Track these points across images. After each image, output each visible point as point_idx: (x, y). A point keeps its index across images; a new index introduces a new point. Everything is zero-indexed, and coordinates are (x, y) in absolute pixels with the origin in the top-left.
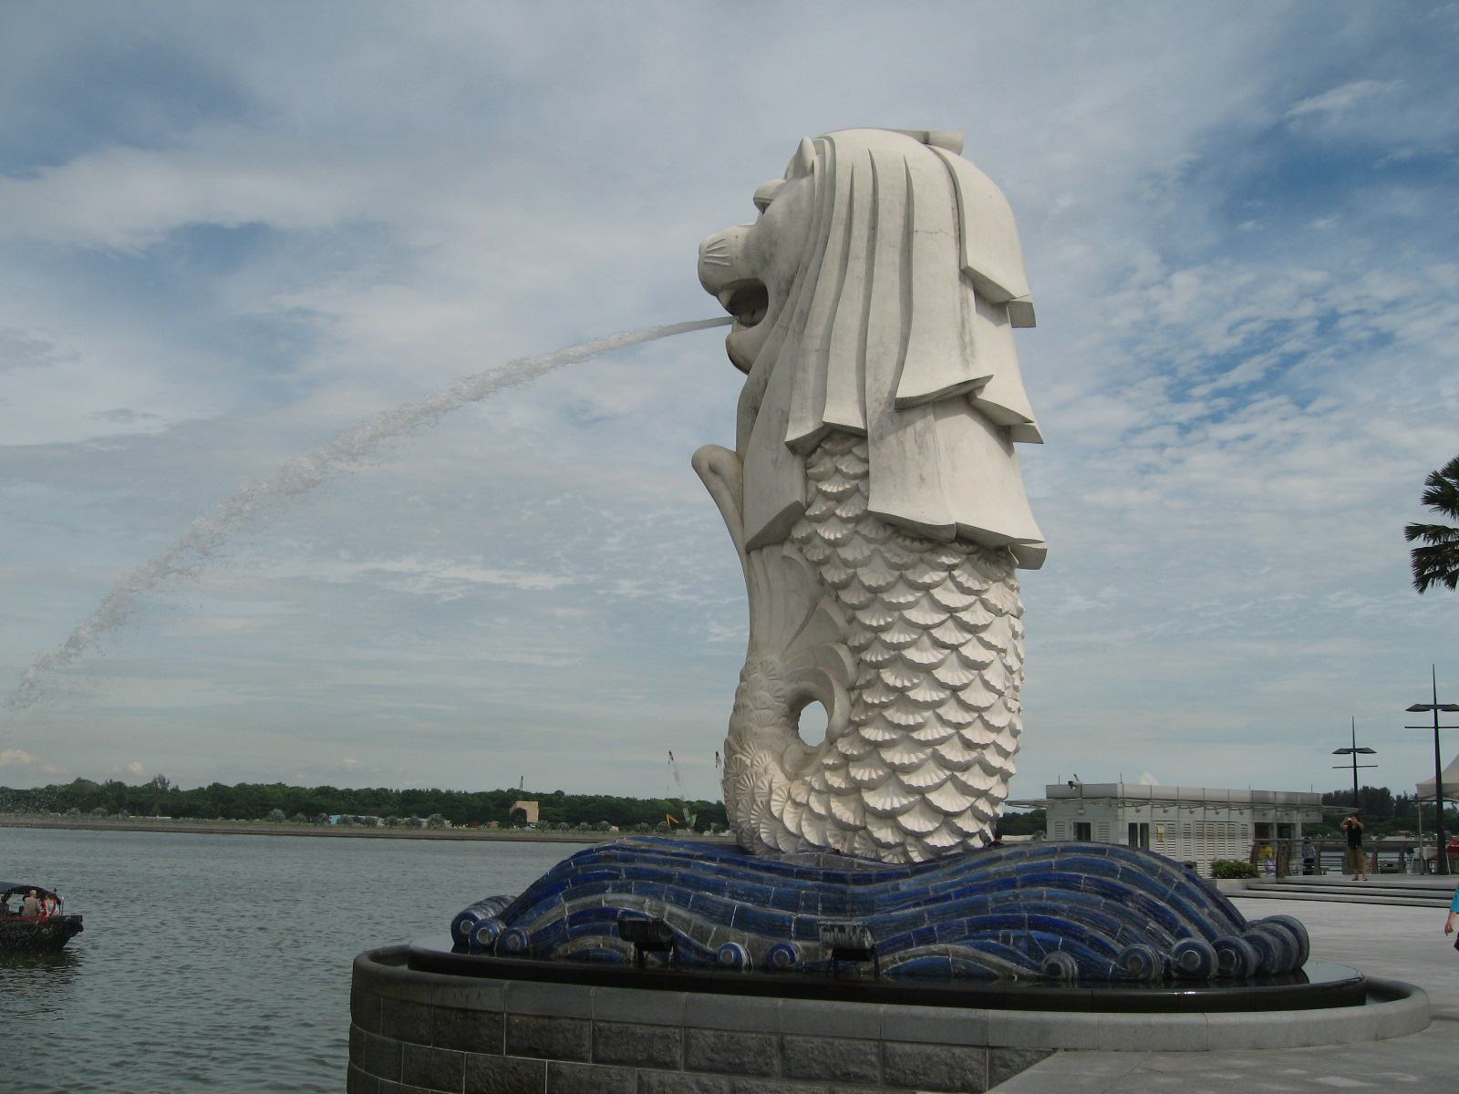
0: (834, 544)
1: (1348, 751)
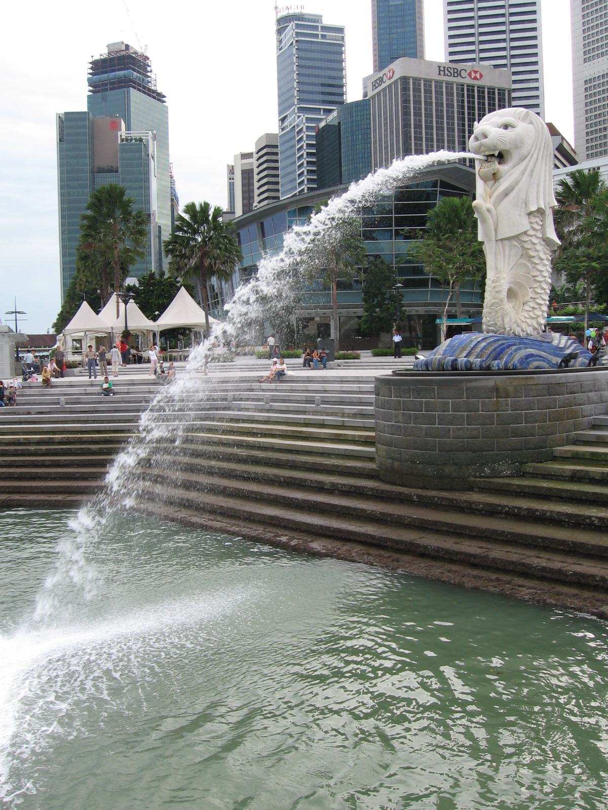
0: (535, 244)
1: (13, 313)
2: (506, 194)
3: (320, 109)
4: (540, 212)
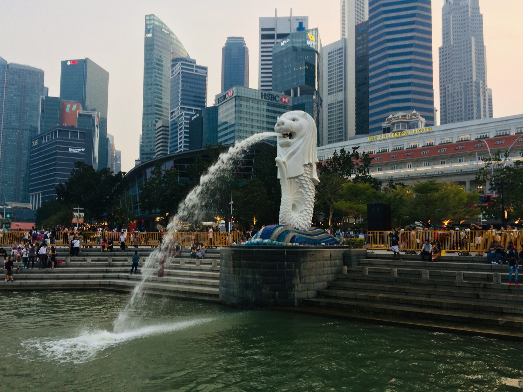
0: (307, 181)
2: (293, 153)
3: (192, 109)
4: (310, 165)
